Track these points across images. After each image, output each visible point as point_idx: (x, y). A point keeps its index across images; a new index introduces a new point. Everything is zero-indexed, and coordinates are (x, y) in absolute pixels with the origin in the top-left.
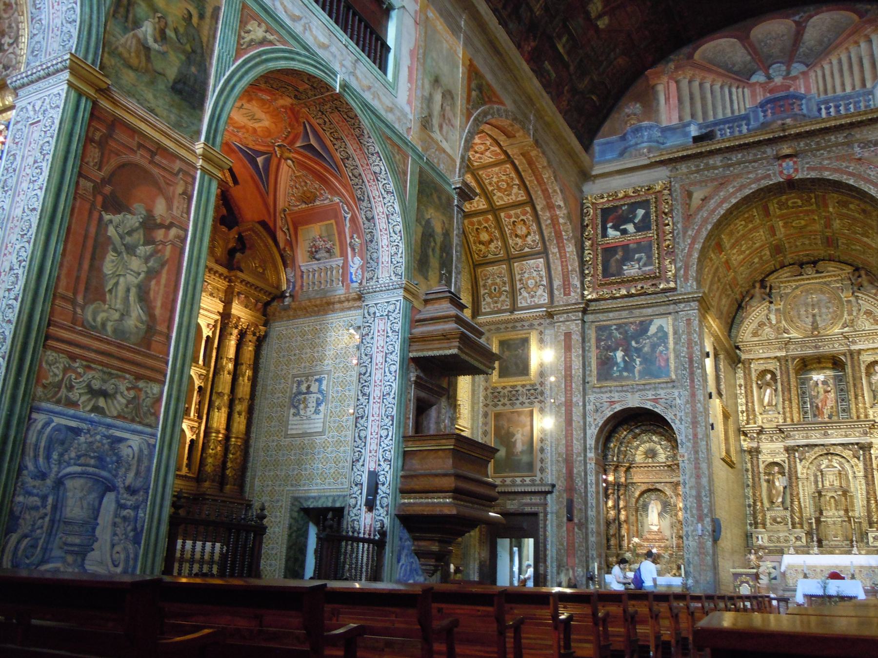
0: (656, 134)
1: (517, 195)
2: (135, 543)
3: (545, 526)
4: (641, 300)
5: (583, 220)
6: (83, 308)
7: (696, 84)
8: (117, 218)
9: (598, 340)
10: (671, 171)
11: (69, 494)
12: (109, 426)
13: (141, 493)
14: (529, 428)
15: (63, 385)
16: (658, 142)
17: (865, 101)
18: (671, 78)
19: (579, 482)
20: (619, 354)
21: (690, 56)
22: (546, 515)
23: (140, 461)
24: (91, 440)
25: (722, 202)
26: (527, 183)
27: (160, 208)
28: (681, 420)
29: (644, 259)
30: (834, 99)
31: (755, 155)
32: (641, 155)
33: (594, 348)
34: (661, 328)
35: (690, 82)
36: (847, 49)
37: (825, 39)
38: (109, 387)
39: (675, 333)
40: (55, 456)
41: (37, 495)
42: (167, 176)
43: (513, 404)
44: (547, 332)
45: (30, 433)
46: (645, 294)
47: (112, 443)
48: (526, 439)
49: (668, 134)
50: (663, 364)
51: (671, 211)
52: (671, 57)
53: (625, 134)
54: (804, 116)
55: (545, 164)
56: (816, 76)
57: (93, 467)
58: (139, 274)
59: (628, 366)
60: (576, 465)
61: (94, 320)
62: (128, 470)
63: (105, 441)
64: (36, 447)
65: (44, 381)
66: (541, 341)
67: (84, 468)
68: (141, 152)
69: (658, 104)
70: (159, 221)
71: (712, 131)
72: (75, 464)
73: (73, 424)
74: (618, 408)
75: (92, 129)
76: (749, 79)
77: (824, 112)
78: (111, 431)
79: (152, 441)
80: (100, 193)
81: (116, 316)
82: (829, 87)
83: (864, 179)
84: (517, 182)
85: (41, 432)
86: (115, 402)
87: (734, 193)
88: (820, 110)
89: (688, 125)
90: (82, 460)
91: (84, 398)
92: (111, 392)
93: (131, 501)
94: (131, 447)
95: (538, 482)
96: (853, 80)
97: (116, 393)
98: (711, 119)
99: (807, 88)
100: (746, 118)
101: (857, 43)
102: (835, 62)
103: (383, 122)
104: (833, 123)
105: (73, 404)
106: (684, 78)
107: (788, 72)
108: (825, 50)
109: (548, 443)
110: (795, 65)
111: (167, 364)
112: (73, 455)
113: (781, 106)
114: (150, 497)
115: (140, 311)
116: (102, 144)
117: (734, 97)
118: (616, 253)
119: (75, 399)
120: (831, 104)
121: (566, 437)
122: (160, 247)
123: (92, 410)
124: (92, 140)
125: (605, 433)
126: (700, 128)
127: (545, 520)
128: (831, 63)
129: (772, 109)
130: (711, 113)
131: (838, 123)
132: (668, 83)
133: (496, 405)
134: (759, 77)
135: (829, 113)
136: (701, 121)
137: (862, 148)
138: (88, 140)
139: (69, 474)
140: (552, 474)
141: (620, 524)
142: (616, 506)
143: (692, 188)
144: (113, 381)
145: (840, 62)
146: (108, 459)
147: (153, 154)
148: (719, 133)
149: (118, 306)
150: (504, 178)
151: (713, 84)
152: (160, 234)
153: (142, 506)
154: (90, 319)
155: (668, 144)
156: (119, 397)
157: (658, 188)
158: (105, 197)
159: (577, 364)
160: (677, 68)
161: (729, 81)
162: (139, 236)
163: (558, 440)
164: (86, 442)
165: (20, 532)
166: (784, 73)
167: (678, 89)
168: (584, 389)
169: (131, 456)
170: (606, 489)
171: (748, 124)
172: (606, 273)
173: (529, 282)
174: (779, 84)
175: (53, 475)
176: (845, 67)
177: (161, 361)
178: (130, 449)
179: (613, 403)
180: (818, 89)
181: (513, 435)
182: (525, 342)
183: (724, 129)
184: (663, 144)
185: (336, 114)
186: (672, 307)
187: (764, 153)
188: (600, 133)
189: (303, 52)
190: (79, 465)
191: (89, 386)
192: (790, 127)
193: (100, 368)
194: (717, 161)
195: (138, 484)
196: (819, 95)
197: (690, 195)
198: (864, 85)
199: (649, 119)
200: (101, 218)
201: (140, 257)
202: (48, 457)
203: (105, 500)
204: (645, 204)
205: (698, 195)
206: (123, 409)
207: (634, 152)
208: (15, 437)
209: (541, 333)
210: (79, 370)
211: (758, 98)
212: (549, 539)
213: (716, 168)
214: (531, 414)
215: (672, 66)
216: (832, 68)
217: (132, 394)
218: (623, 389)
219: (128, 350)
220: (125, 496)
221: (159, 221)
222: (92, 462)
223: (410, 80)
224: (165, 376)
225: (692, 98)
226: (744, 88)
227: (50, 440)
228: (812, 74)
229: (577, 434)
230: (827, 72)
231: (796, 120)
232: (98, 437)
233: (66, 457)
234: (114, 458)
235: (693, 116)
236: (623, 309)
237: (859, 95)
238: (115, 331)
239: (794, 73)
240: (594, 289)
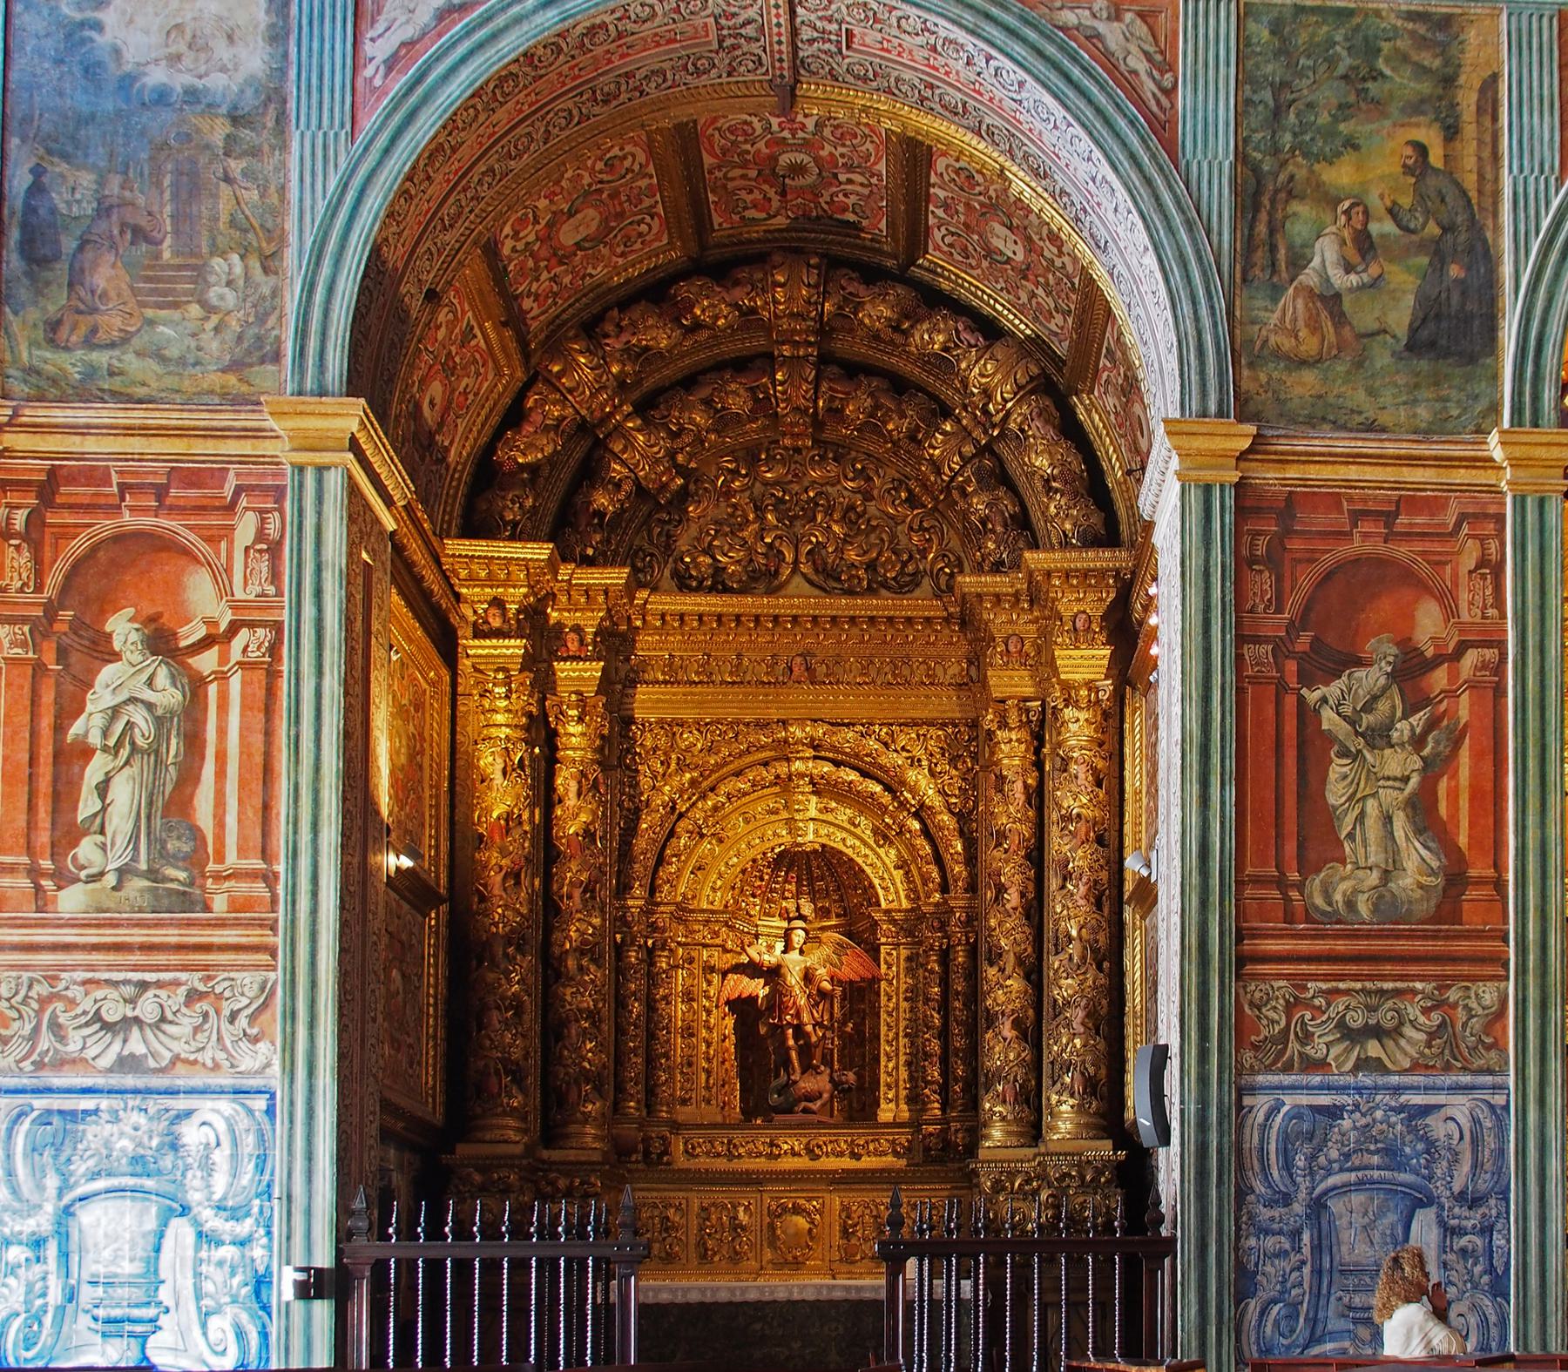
2: (1495, 1296)
6: (1300, 887)
8: (1334, 689)
11: (1342, 1223)
12: (1397, 1090)
13: (1492, 1202)
15: (1292, 1036)
23: (1476, 1142)
24: (1363, 1121)
27: (1428, 624)
38: (1386, 1017)
40: (1300, 1161)
41: (1280, 1233)
42: (1428, 546)
45: (1247, 1131)
47: (1411, 1118)
57: (1379, 1168)
58: (1406, 780)
61: (1329, 900)
62: (1455, 1159)
63: (1393, 1119)
64: (1262, 1151)
65: (1253, 1038)
67: (1360, 1174)
68: (1366, 527)
70: (1429, 653)
72: (1341, 1170)
73: (1324, 1100)
75: (1246, 539)
78: (1403, 1099)
79: (1499, 1100)
80: (1291, 655)
81: (1374, 878)
85: (1264, 1127)
86: (1403, 1042)
90: (1356, 1160)
91: (1334, 1051)
92: (1388, 1025)
93: (1473, 1219)
94: (1452, 1119)
97: (1401, 1024)
105: (1321, 1065)
111: (1505, 940)
112: (1334, 1154)
114: (1512, 1207)
115: (1424, 852)
116: (1273, 561)
119: (1319, 1055)
122: (1443, 707)
123: (1357, 1068)
124: (1253, 560)
138: (1243, 563)
139: (1335, 1188)
144: (1390, 1004)
146: (1408, 1150)
147: (1389, 518)
149: (1372, 860)
152: (1439, 678)
153: (1499, 1226)
154: (1319, 901)
156: (1408, 1031)
158: (1302, 658)
162: (1394, 701)
164: (1355, 1128)
165: (1263, 1295)
169: (1457, 1136)
175: (1302, 1195)
177: (1493, 938)
178: (1451, 1124)
190: (1351, 1170)
191: (1341, 1024)
193: (1358, 985)
195: (1484, 1183)
200: (1301, 701)
201: (1402, 745)
202: (1288, 1166)
203: (1415, 1226)
206: (1422, 1054)
208: (1220, 1144)
210: (1317, 1002)
217: (1436, 1017)
219: (1408, 938)
220: (1457, 1210)
221: (1429, 653)
222: (1376, 1159)
224: (1506, 965)
227: (1286, 1139)
232: (1379, 1114)
233: (1322, 1160)
234: (1420, 1146)
238: (1376, 909)
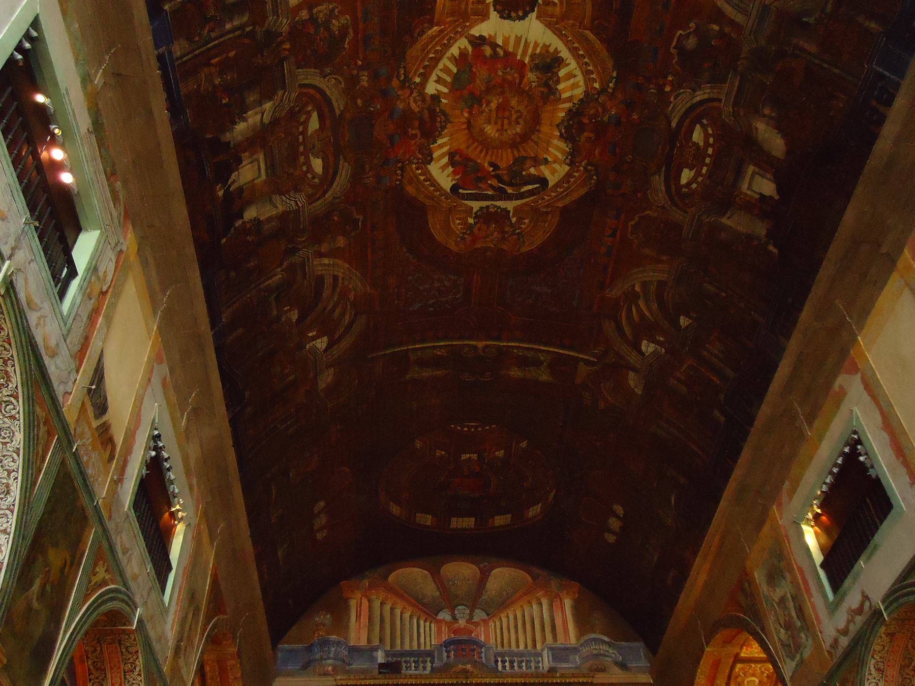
7: (387, 607)
16: (343, 661)
17: (535, 662)
21: (386, 578)
30: (512, 654)
32: (326, 674)
35: (382, 603)
36: (522, 606)
37: (505, 593)
52: (367, 573)
53: (311, 646)
54: (482, 664)
55: (239, 675)
56: (495, 626)
76: (437, 615)
82: (506, 641)
89: (375, 649)
96: (526, 638)
98: (398, 648)
99: (487, 636)
100: (430, 654)
101: (530, 602)
102: (511, 617)
108: (502, 604)
113: (463, 650)
117: (422, 630)
120: (507, 658)
128: (508, 617)
130: (398, 642)
132: (361, 598)
134: (445, 615)
135: (504, 667)
136: (388, 648)
145: (515, 618)
148: (404, 665)
151: (404, 613)
155: (353, 666)
160: (371, 587)
166: (467, 617)
167: (370, 607)
171: (432, 662)
174: (462, 626)
180: (496, 640)
183: (409, 662)
184: (350, 664)
189: (123, 589)
192: (472, 675)
196: (497, 647)
198: (535, 646)
211: (443, 636)
215: (366, 582)
216: (508, 621)
223: (177, 604)
225: (382, 621)
226: (431, 623)
228: (491, 624)
230: (505, 626)
231: (474, 667)
235: (381, 640)
237: (530, 654)
239: (476, 619)
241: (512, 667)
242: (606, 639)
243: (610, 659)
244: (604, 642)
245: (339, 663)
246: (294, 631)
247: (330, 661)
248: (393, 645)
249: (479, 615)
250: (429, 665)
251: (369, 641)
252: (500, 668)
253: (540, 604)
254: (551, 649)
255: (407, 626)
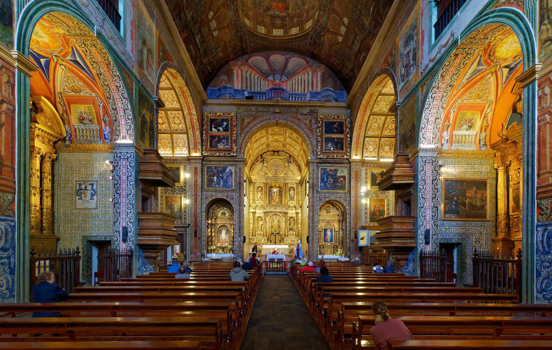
0: (233, 92)
1: (176, 105)
3: (186, 238)
4: (224, 159)
5: (202, 122)
7: (248, 74)
9: (207, 172)
10: (237, 109)
14: (180, 203)
18: (239, 68)
19: (199, 224)
20: (215, 178)
21: (247, 61)
22: (186, 235)
25: (254, 126)
26: (181, 101)
28: (235, 204)
29: (226, 143)
30: (295, 94)
31: (267, 110)
33: (206, 175)
34: (230, 170)
36: (301, 75)
39: (235, 173)
43: (173, 193)
44: (187, 166)
46: (225, 156)
48: (179, 207)
49: (237, 92)
50: (230, 183)
51: (236, 125)
52: (240, 58)
59: (218, 183)
60: (198, 217)
66: (185, 169)
69: (234, 78)
71: (253, 96)
74: (214, 198)
77: (291, 98)
83: (300, 127)
84: (176, 99)
87: (258, 123)
88: (289, 97)
89: (244, 91)
95: (183, 223)
98: (253, 91)
100: (264, 93)
101: (304, 73)
103: (120, 60)
104: (293, 104)
106: (244, 70)
107: (281, 79)
109: (187, 209)
110: (283, 76)
117: (262, 84)
118: (215, 138)
121: (195, 207)
125: (208, 207)
126: (249, 93)
127: (186, 236)
129: (274, 92)
130: (253, 88)
131: (295, 104)
133: (166, 193)
134: (271, 78)
135: (292, 99)
136: (249, 90)
137: (301, 115)
140: (189, 220)
141: (212, 237)
142: (211, 232)
143: (244, 118)
150: (170, 96)
151: (255, 76)
157: (232, 115)
159: (199, 180)
160: (242, 65)
161: (261, 76)
163: (192, 208)
168: (202, 190)
170: (208, 225)
171: (265, 96)
172: (211, 146)
173: (180, 144)
176: (300, 82)
179: (212, 196)
181: (173, 205)
182: (178, 169)
184: (235, 96)
185: (94, 48)
186: (234, 163)
187: (270, 109)
188: (209, 86)
194: (253, 108)
197: (243, 120)
198: (304, 91)
199: (230, 84)
204: (227, 121)
205: (246, 121)
207: (223, 97)
209: (185, 166)
212: (188, 243)
213: (253, 111)
214: (181, 198)
218: (216, 191)
225: (246, 80)
228: (289, 82)
229: (199, 206)
231: (281, 99)
235: (246, 87)
236: (217, 161)
237: (302, 95)
239: (283, 80)
240: (206, 151)
241: (295, 99)
242: (332, 89)
243: (332, 97)
244: (331, 91)
245: (231, 96)
246: (213, 83)
247: (228, 95)
248: (251, 89)
249: (284, 78)
250: (264, 97)
251: (242, 87)
252: (291, 100)
253: (309, 74)
254: (311, 93)
255: (256, 82)
